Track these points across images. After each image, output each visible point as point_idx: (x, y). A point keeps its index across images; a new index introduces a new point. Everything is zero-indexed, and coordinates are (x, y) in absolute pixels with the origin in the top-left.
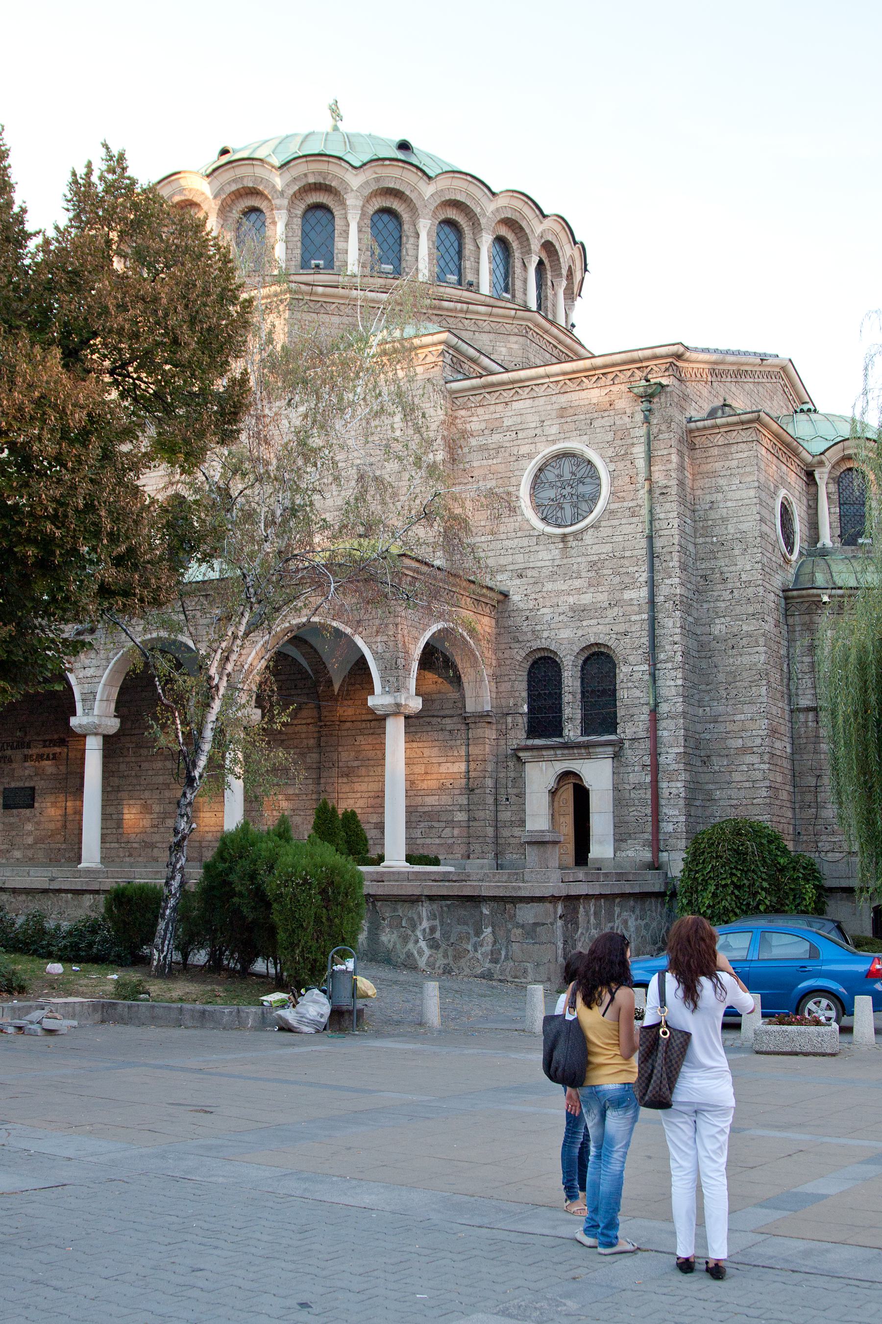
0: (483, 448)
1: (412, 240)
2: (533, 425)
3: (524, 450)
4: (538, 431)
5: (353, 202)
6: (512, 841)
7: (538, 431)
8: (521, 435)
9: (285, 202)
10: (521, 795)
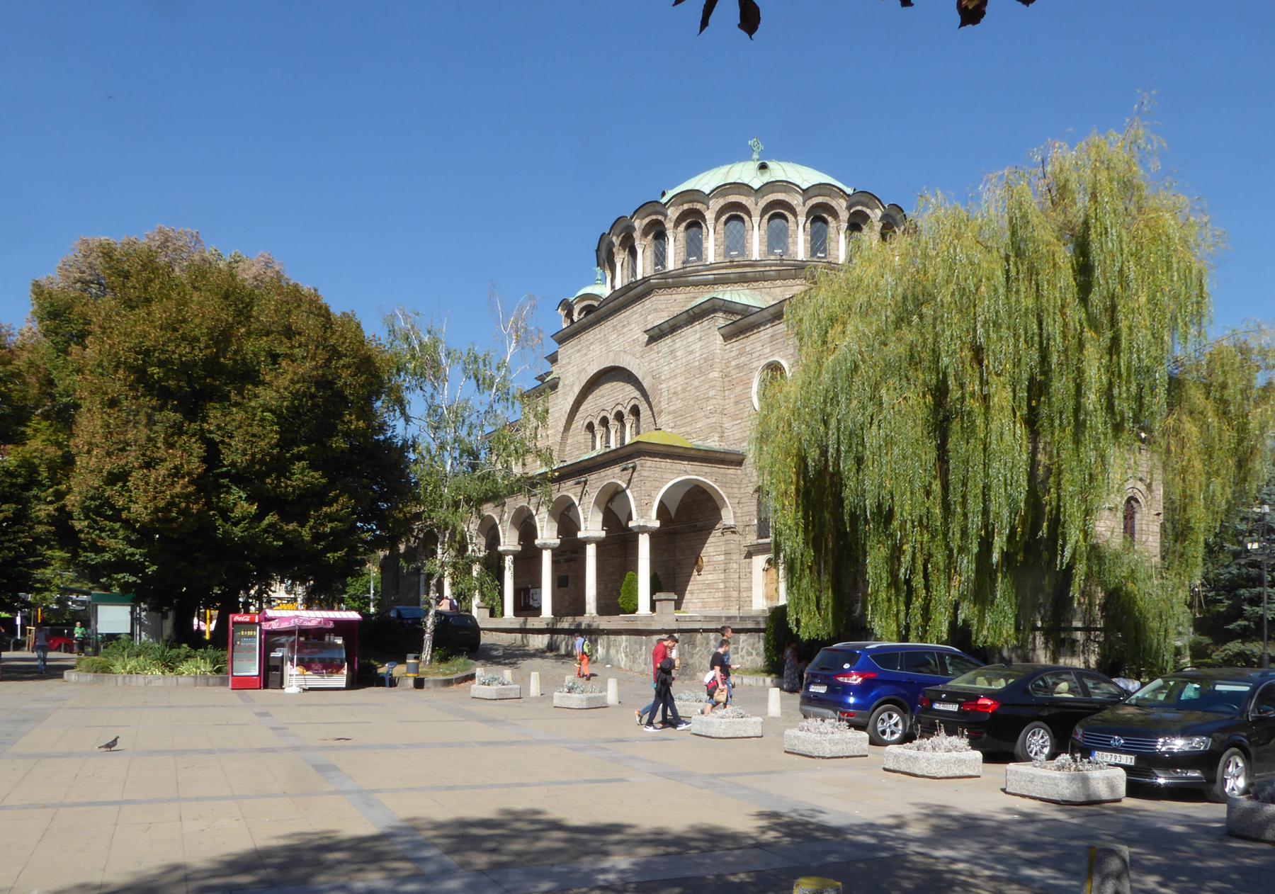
0: (737, 366)
1: (750, 232)
2: (759, 349)
3: (755, 365)
4: (761, 352)
5: (710, 216)
6: (747, 599)
7: (761, 352)
8: (754, 356)
9: (672, 224)
10: (750, 573)
